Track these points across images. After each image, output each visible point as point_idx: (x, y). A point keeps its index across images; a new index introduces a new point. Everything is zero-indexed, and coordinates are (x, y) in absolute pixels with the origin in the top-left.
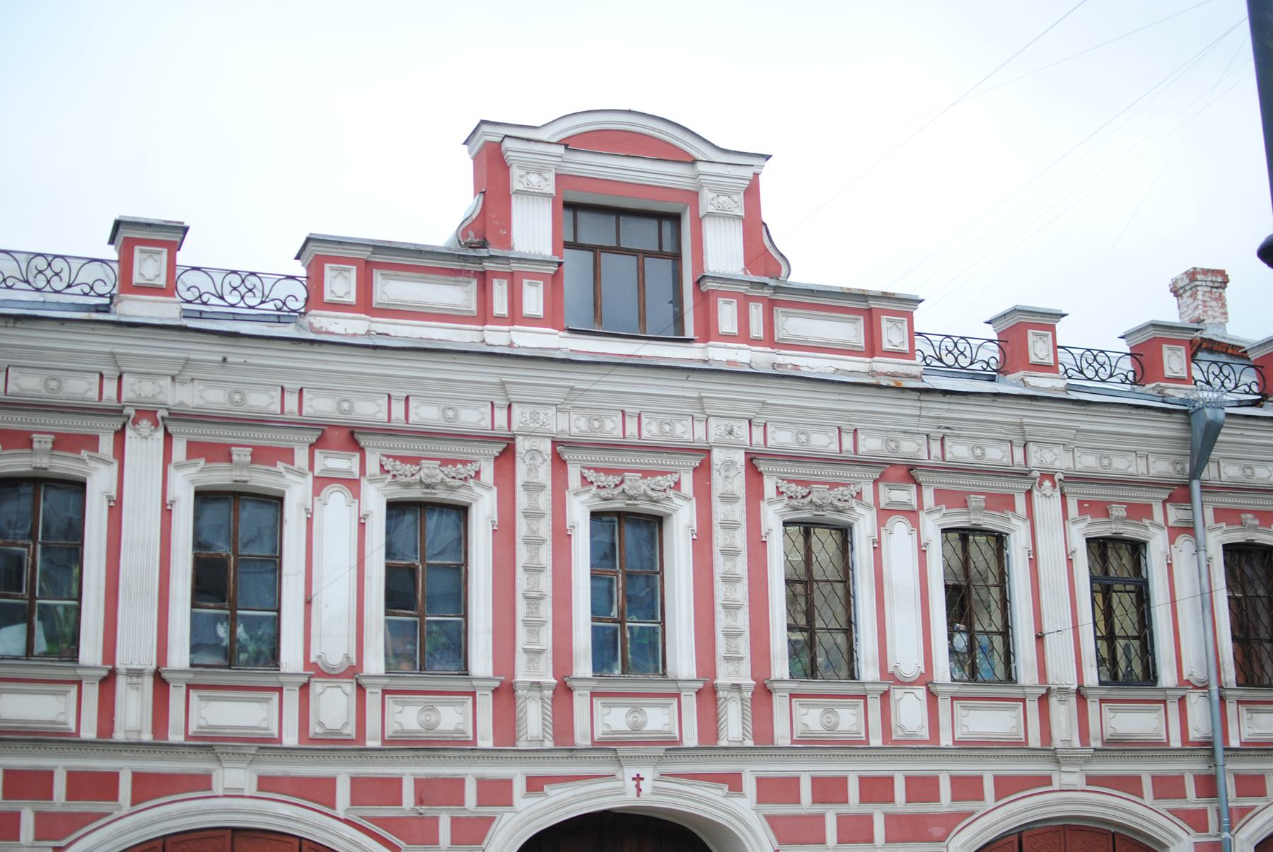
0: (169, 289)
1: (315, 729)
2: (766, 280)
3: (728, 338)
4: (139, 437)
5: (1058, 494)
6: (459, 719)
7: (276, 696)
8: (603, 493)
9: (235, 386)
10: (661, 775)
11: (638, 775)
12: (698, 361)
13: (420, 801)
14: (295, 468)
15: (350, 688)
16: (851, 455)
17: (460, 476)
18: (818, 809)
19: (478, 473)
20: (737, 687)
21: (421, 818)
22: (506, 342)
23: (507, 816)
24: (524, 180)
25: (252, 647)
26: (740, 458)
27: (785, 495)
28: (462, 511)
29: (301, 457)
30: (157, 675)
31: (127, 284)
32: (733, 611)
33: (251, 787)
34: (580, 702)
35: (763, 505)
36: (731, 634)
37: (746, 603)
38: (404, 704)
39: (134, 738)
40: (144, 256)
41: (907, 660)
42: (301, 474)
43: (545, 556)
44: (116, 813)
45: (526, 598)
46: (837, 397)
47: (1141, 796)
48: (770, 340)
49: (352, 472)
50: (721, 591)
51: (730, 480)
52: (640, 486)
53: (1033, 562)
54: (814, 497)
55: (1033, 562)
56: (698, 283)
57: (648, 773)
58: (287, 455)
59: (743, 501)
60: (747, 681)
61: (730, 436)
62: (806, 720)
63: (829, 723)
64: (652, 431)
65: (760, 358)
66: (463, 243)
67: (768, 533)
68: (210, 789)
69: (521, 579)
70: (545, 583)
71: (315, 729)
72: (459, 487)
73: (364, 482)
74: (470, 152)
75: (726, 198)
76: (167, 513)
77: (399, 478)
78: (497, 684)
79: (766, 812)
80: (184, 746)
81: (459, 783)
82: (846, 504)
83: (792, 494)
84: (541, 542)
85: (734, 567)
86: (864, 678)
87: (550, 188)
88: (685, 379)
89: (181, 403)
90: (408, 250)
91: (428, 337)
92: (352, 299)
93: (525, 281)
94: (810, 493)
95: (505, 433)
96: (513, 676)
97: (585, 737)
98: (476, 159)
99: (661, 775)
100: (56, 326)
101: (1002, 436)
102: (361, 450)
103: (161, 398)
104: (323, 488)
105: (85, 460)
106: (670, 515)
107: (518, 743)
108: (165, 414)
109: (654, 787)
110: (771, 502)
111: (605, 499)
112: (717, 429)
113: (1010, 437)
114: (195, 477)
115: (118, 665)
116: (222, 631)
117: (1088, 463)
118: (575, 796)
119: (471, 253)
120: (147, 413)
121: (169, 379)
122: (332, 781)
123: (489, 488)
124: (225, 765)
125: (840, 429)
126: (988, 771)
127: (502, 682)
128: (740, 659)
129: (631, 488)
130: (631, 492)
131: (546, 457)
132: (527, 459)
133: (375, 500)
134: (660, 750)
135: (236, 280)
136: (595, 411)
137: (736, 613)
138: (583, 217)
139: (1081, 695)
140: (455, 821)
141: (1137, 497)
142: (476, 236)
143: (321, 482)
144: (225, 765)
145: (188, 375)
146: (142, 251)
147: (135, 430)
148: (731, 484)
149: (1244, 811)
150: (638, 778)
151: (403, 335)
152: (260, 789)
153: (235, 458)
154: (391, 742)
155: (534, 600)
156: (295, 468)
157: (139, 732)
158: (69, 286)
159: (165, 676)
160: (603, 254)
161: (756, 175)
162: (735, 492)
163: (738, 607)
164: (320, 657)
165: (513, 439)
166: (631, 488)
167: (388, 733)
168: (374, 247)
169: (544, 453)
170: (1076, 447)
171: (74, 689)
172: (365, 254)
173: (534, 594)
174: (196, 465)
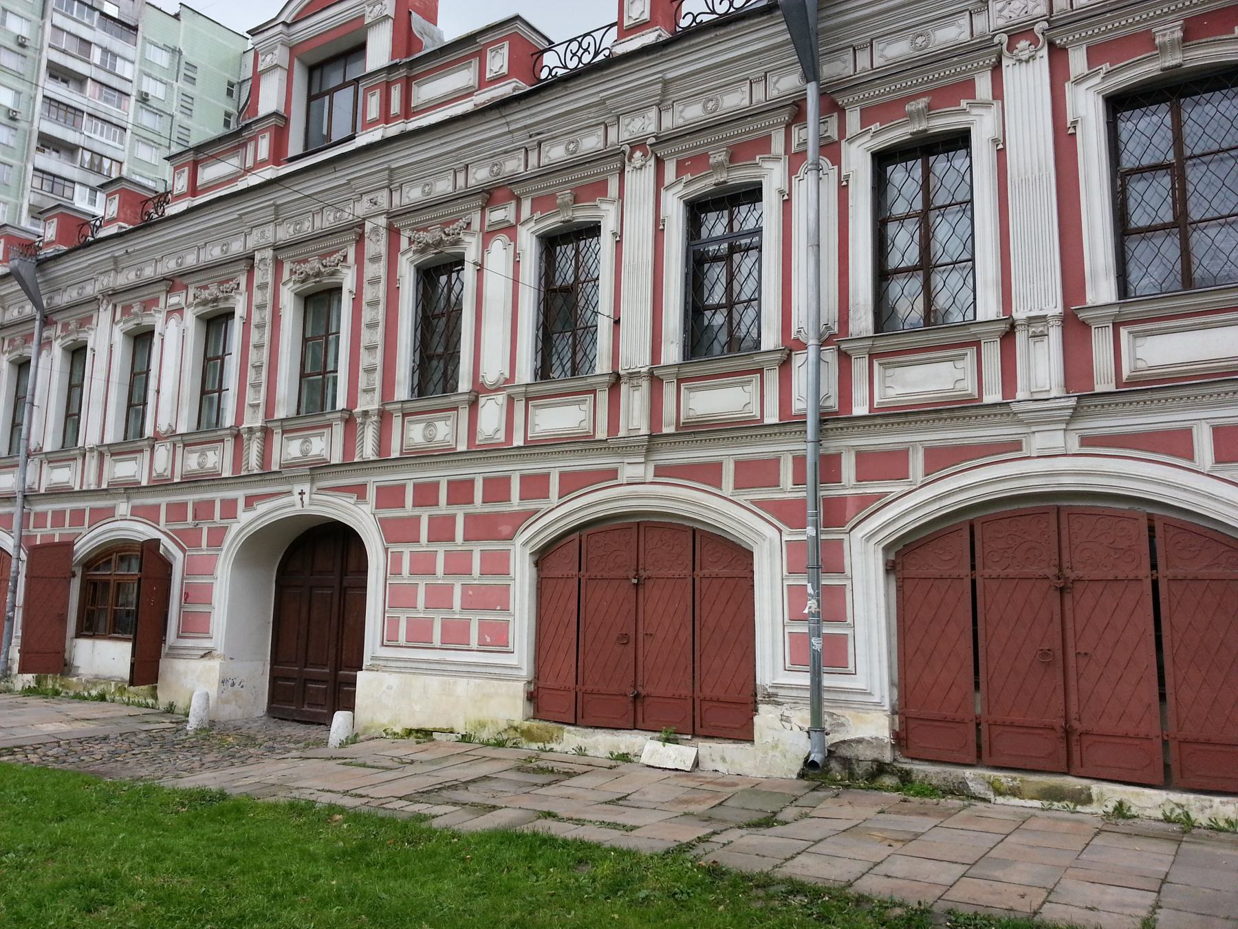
5: (652, 162)
13: (195, 517)
26: (382, 221)
41: (493, 370)
46: (438, 142)
47: (718, 485)
48: (408, 112)
53: (619, 244)
55: (619, 244)
57: (306, 488)
65: (393, 130)
71: (154, 474)
97: (276, 464)
101: (593, 121)
113: (601, 119)
117: (693, 113)
126: (554, 468)
133: (190, 316)
139: (655, 381)
141: (749, 132)
143: (170, 313)
149: (865, 501)
150: (302, 493)
155: (258, 368)
166: (311, 269)
170: (674, 102)
173: (258, 364)
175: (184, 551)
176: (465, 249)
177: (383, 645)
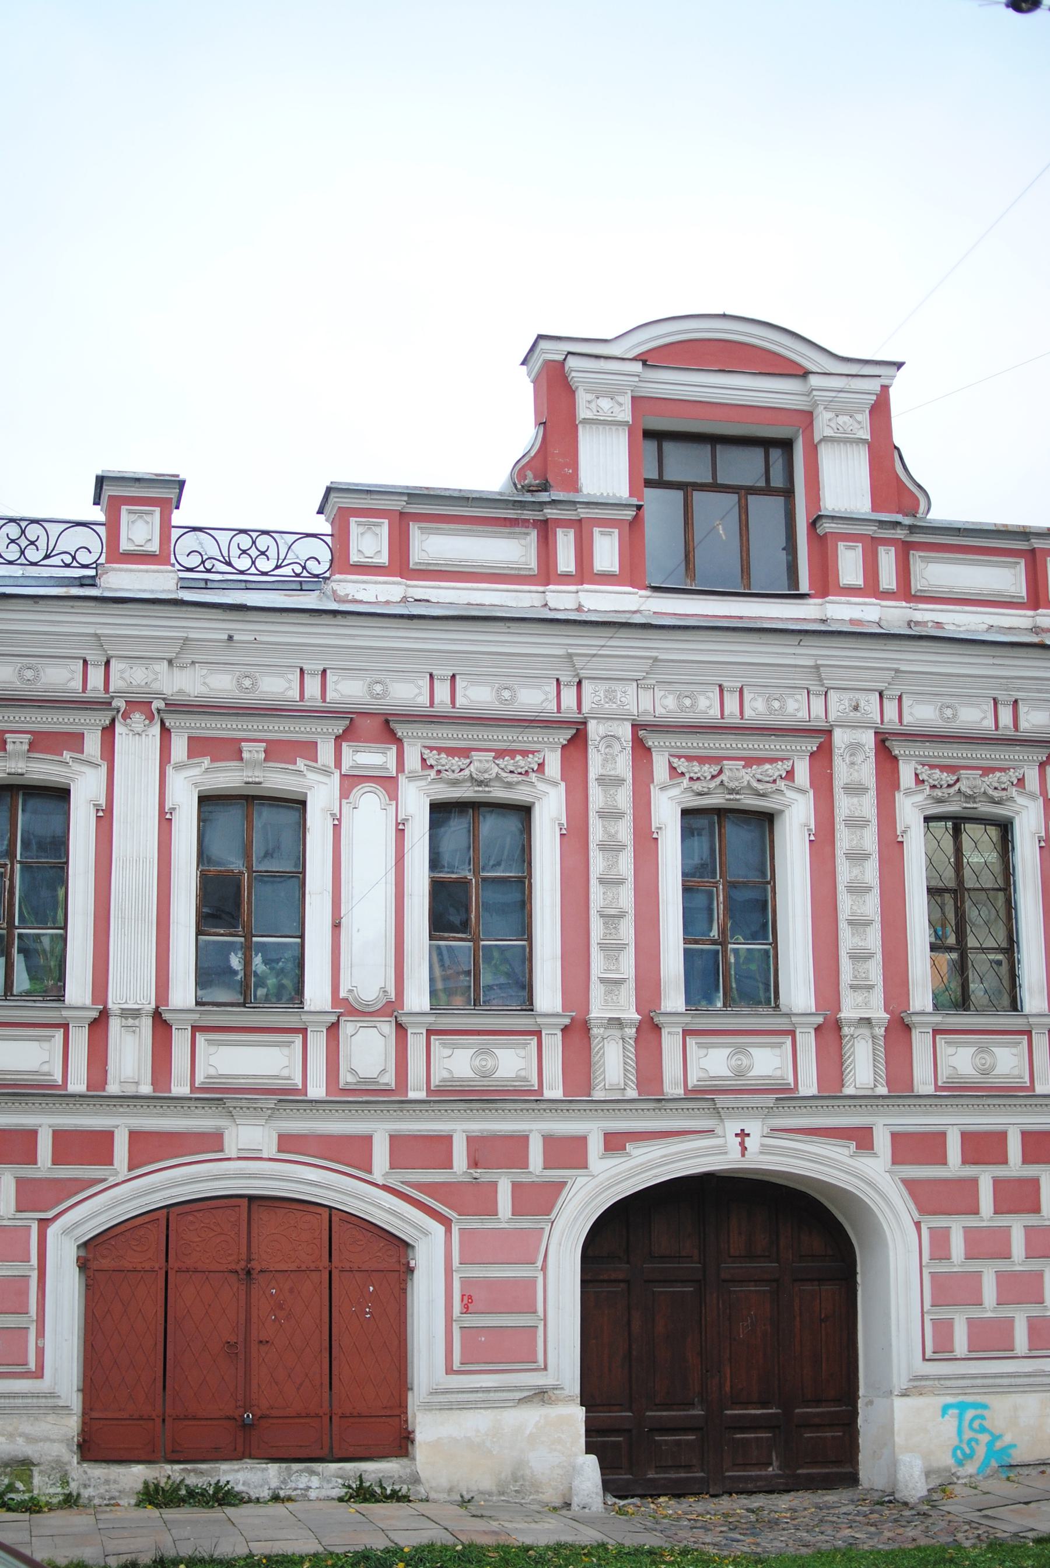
0: (161, 557)
1: (346, 1078)
2: (899, 518)
3: (851, 591)
4: (131, 733)
6: (521, 1064)
7: (298, 1039)
8: (697, 786)
9: (244, 669)
10: (771, 1130)
11: (743, 1130)
12: (815, 621)
13: (474, 1163)
14: (319, 765)
15: (388, 1028)
16: (1011, 733)
17: (520, 770)
18: (970, 1171)
19: (541, 766)
20: (867, 1021)
21: (475, 1183)
22: (573, 605)
23: (581, 1181)
24: (593, 406)
25: (271, 981)
26: (868, 739)
27: (926, 783)
28: (524, 812)
29: (326, 752)
30: (157, 1015)
31: (116, 554)
32: (861, 929)
33: (270, 1149)
34: (671, 1042)
35: (899, 797)
36: (859, 957)
37: (878, 918)
38: (455, 1046)
39: (130, 1090)
40: (133, 517)
42: (326, 772)
43: (625, 865)
44: (111, 1179)
45: (602, 916)
46: (991, 661)
48: (905, 592)
49: (387, 769)
50: (846, 905)
51: (856, 767)
52: (743, 777)
54: (963, 786)
56: (813, 525)
57: (755, 1128)
58: (309, 750)
59: (873, 793)
60: (880, 1014)
61: (855, 713)
62: (954, 1061)
63: (983, 1065)
64: (757, 709)
66: (519, 487)
67: (904, 832)
68: (222, 1150)
69: (597, 895)
70: (626, 898)
71: (346, 1078)
72: (518, 783)
73: (402, 779)
74: (529, 375)
75: (846, 418)
76: (165, 821)
77: (444, 775)
78: (567, 1021)
79: (904, 1175)
80: (190, 1099)
81: (522, 1141)
82: (1004, 793)
83: (936, 783)
84: (621, 847)
85: (863, 873)
86: (1027, 1010)
87: (625, 415)
88: (797, 644)
89: (180, 692)
90: (451, 497)
91: (478, 602)
92: (384, 559)
93: (596, 531)
94: (958, 780)
95: (574, 716)
96: (588, 1011)
97: (676, 1084)
98: (535, 382)
99: (771, 1130)
100: (28, 605)
102: (399, 742)
103: (156, 686)
104: (353, 788)
105: (68, 763)
106: (782, 812)
107: (593, 1093)
108: (161, 705)
109: (762, 1145)
110: (909, 793)
111: (700, 794)
112: (839, 705)
114: (198, 779)
115: (110, 1005)
116: (235, 962)
118: (665, 1156)
119: (528, 497)
120: (139, 704)
121: (166, 663)
122: (366, 1141)
123: (555, 784)
124: (238, 1121)
125: (995, 701)
127: (573, 1019)
128: (870, 987)
129: (731, 779)
130: (732, 785)
131: (624, 743)
132: (602, 748)
134: (769, 1100)
135: (245, 541)
136: (685, 686)
137: (865, 931)
138: (668, 447)
140: (516, 1186)
142: (535, 478)
143: (350, 782)
144: (238, 1121)
145: (188, 658)
146: (130, 512)
147: (126, 725)
148: (858, 771)
150: (743, 1134)
151: (447, 601)
152: (280, 1150)
153: (245, 755)
154: (439, 1092)
155: (611, 919)
156: (319, 765)
157: (137, 1083)
158: (47, 557)
159: (166, 1016)
160: (695, 493)
161: (885, 388)
162: (863, 782)
163: (868, 923)
164: (350, 991)
165: (585, 723)
166: (731, 779)
167: (435, 1081)
168: (409, 495)
169: (623, 740)
171: (59, 1034)
172: (398, 504)
173: (613, 912)
174: (199, 764)
175: (446, 1222)
176: (1018, 813)
177: (924, 1359)
